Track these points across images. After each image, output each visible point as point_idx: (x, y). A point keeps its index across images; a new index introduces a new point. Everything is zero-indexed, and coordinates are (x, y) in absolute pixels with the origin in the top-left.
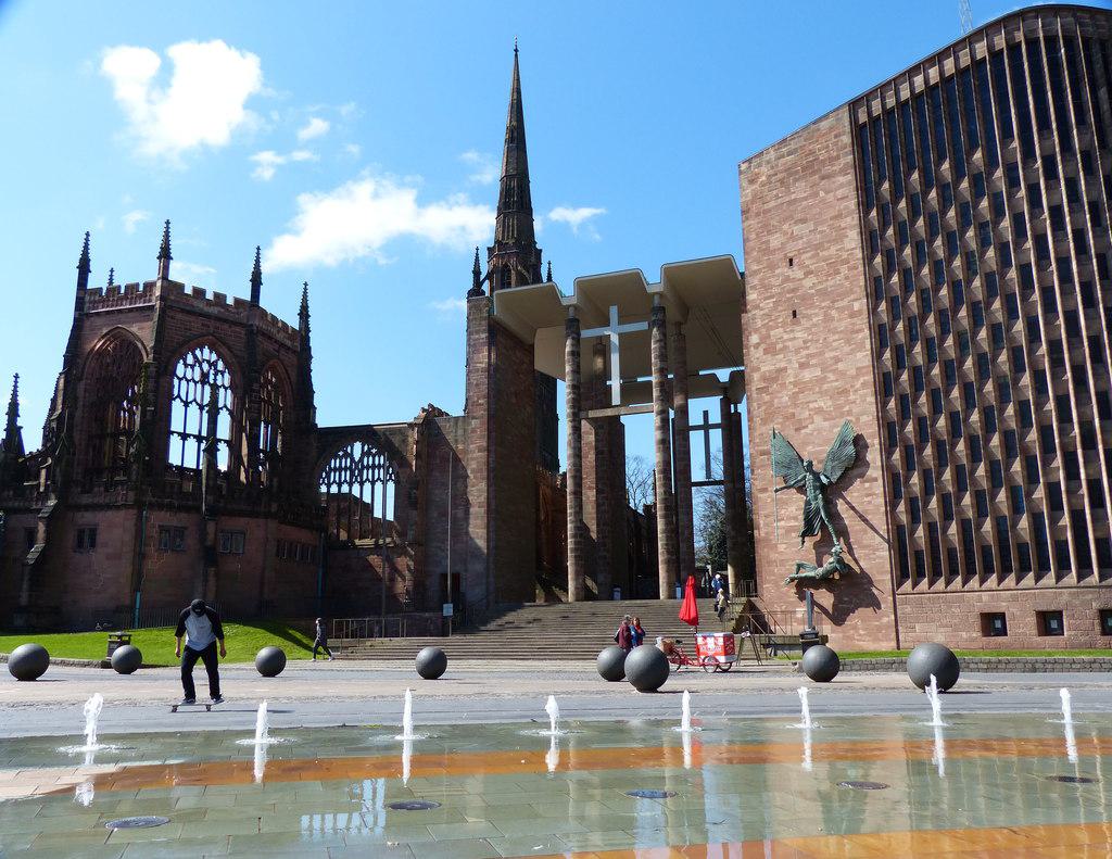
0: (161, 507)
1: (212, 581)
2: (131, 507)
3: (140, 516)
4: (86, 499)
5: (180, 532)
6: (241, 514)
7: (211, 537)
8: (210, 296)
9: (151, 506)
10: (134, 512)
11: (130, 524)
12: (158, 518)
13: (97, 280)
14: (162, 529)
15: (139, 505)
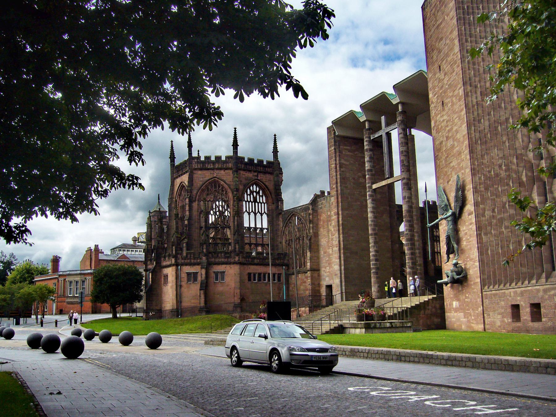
0: (186, 264)
1: (203, 296)
2: (173, 265)
3: (177, 270)
4: (164, 264)
5: (195, 274)
6: (223, 263)
7: (204, 276)
8: (213, 159)
9: (182, 265)
10: (174, 268)
11: (174, 273)
12: (188, 269)
13: (177, 163)
14: (189, 274)
15: (177, 265)
